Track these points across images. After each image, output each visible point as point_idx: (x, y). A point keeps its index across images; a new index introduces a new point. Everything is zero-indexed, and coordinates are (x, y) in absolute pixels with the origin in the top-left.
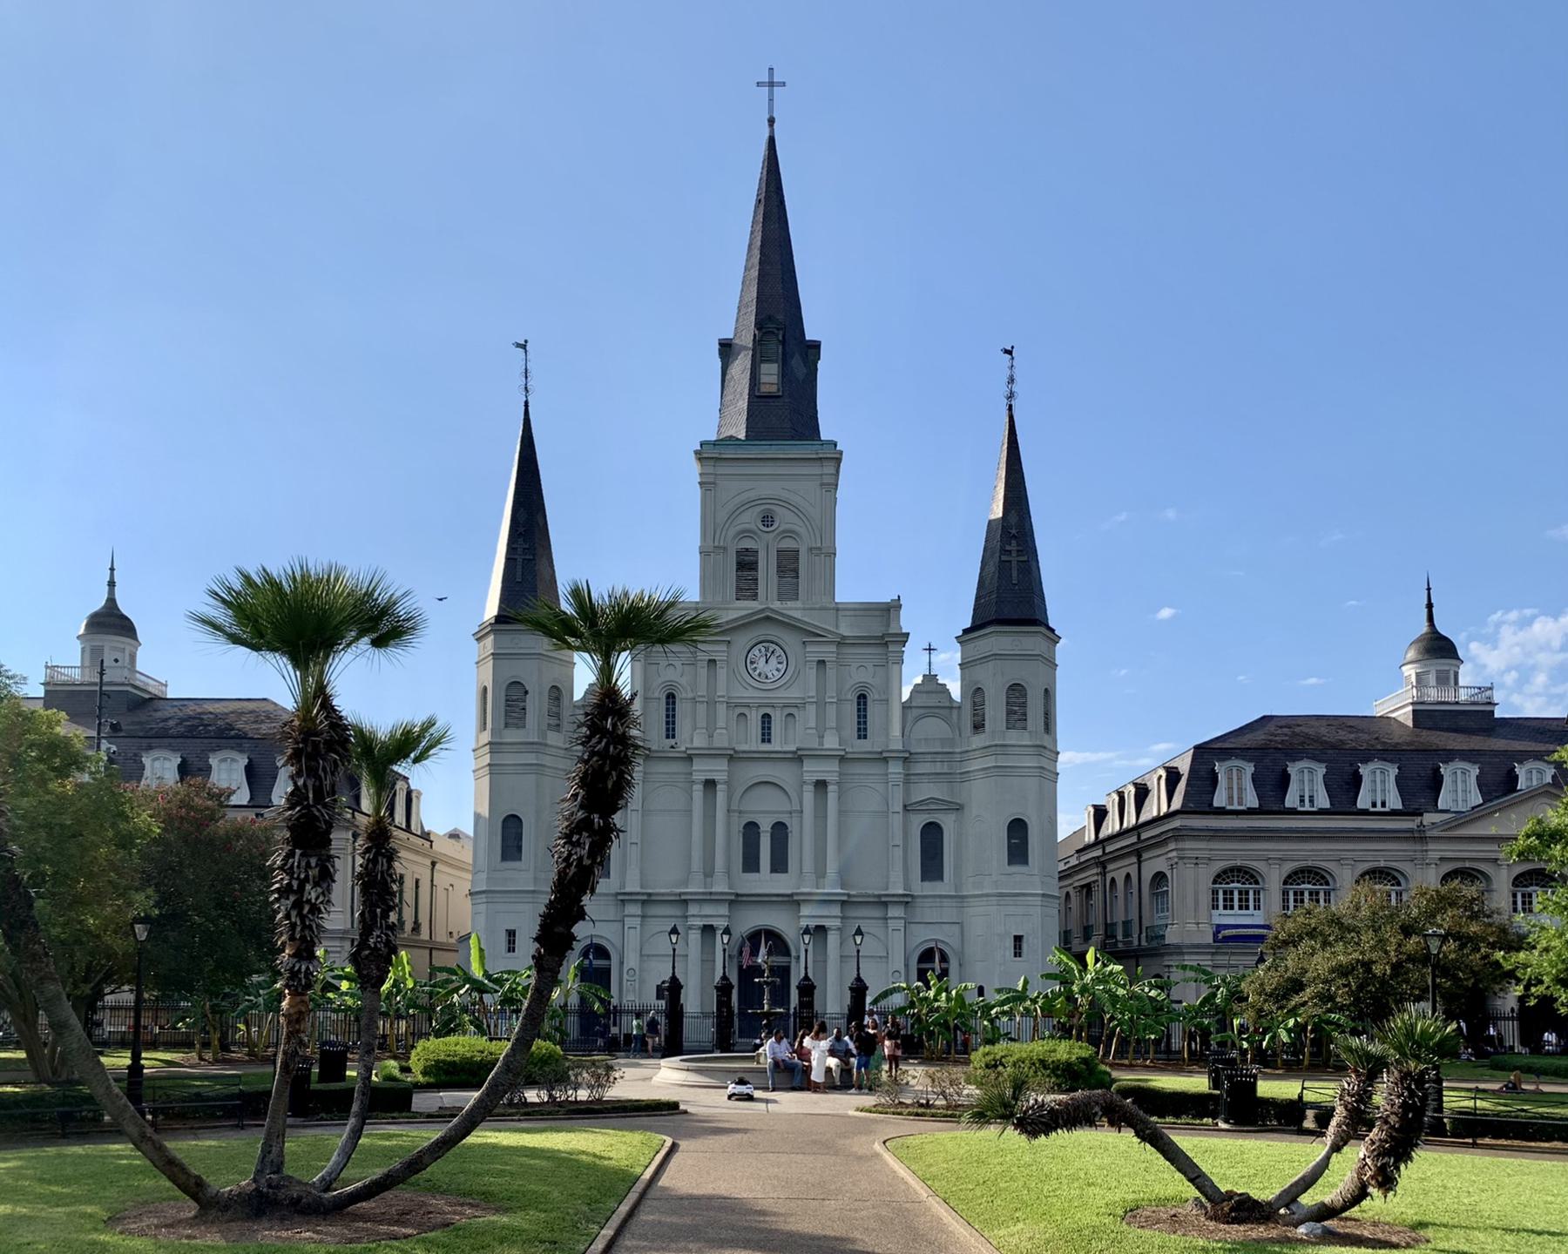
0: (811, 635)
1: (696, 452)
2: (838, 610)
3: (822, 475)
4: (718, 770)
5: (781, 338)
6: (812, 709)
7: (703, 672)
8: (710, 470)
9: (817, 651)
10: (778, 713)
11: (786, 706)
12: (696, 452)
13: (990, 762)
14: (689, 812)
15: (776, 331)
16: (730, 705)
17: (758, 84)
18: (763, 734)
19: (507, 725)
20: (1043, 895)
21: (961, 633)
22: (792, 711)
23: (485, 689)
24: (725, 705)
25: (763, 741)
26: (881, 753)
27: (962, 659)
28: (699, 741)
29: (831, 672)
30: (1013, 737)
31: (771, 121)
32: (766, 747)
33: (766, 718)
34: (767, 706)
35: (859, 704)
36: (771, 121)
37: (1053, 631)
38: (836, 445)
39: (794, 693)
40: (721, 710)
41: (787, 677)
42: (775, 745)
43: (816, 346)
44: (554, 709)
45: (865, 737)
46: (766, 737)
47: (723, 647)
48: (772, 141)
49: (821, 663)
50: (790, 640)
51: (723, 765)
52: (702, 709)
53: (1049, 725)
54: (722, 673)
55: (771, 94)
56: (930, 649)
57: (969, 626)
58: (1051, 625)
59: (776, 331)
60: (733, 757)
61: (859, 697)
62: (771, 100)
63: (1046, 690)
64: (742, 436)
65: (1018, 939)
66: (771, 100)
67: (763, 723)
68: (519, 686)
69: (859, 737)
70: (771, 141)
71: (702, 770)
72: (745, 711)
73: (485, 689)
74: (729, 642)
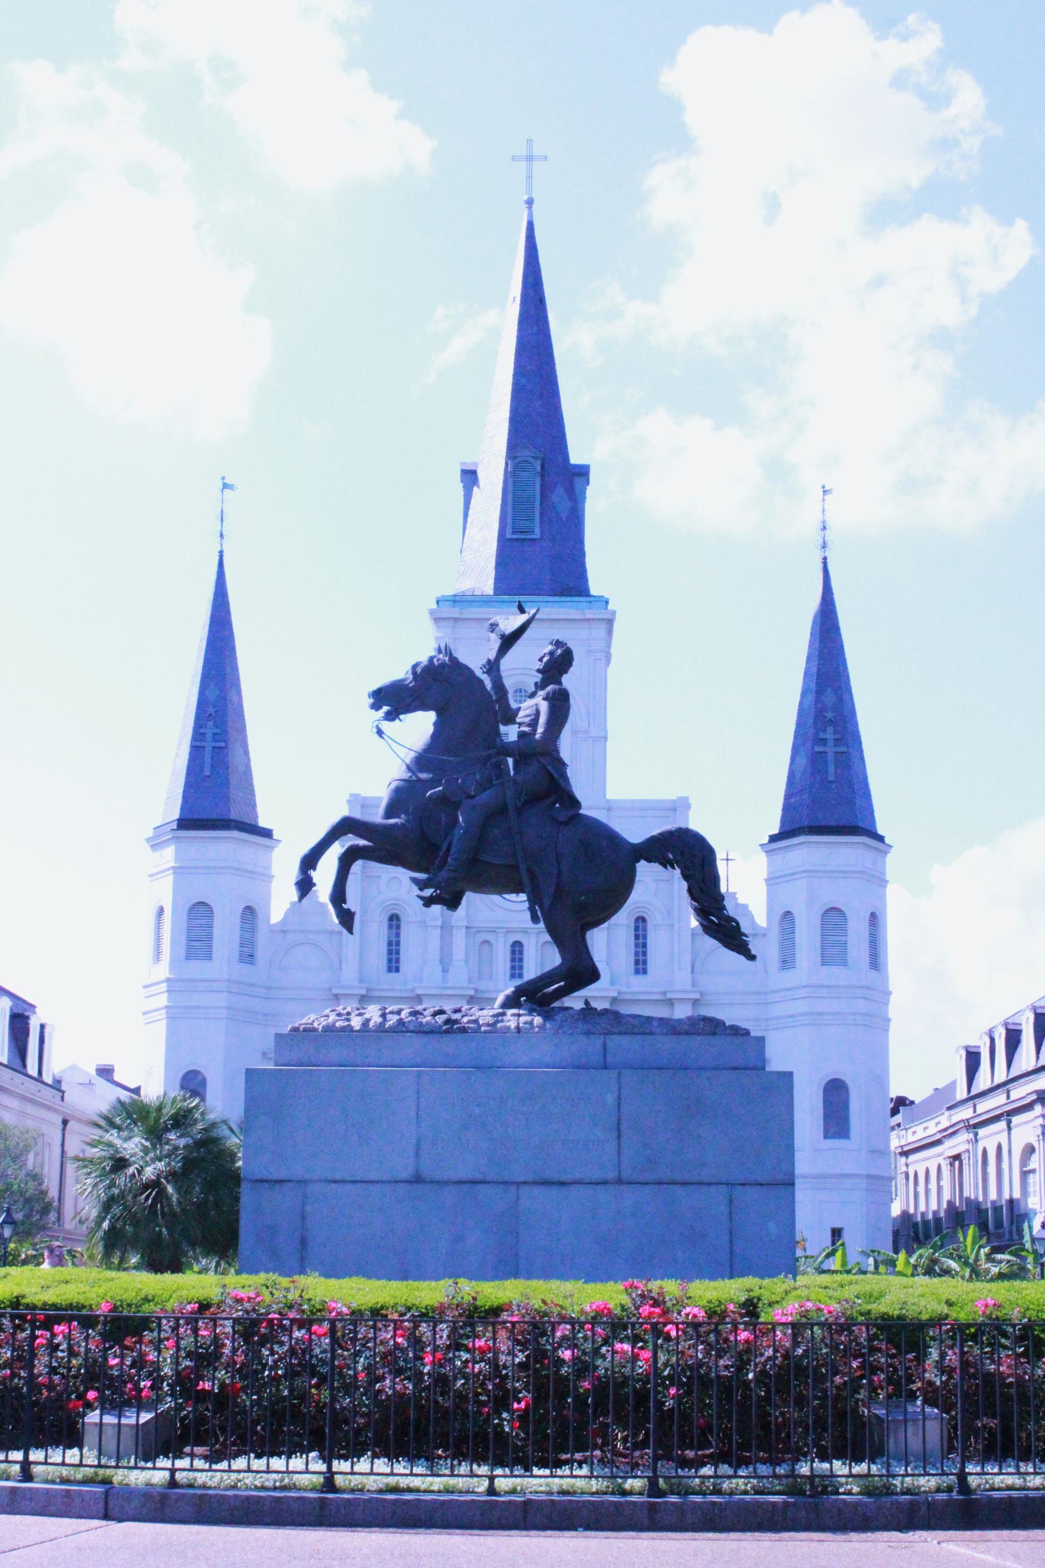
3: (588, 639)
5: (539, 468)
13: (802, 1006)
15: (531, 460)
17: (514, 158)
18: (513, 968)
19: (188, 957)
20: (868, 1176)
21: (766, 840)
23: (161, 911)
24: (464, 930)
26: (665, 993)
27: (769, 873)
30: (834, 975)
31: (530, 203)
35: (636, 928)
36: (530, 203)
37: (881, 839)
38: (607, 602)
43: (583, 472)
44: (247, 935)
45: (645, 972)
48: (530, 227)
53: (876, 959)
56: (727, 860)
57: (776, 831)
58: (880, 832)
59: (531, 460)
61: (637, 920)
62: (529, 177)
64: (490, 590)
65: (836, 1233)
66: (529, 177)
67: (513, 952)
68: (201, 908)
69: (637, 972)
70: (530, 227)
72: (489, 937)
73: (161, 911)
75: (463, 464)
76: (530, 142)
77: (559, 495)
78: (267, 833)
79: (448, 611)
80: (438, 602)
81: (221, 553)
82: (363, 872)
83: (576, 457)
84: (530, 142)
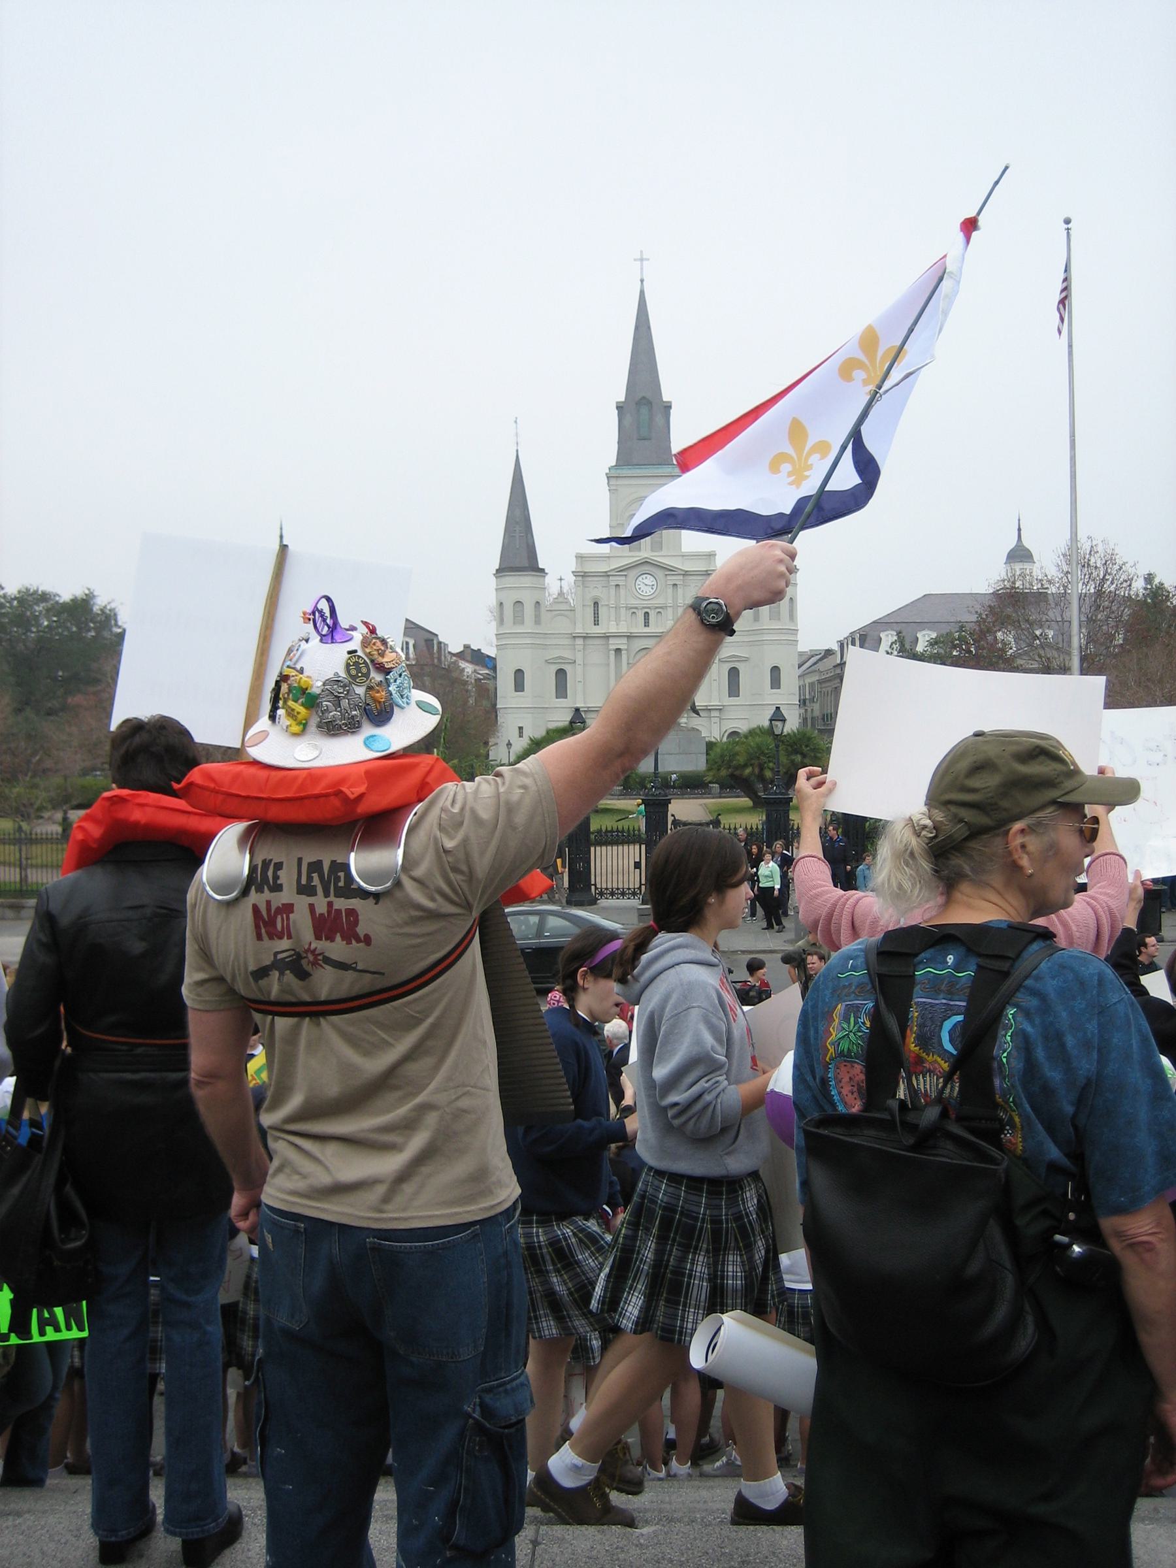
0: (668, 570)
1: (607, 474)
2: (683, 556)
4: (622, 643)
6: (670, 610)
7: (613, 591)
8: (613, 482)
9: (672, 579)
10: (653, 611)
11: (657, 608)
12: (607, 474)
14: (608, 665)
16: (628, 608)
17: (635, 260)
19: (514, 623)
22: (660, 609)
25: (645, 626)
28: (613, 629)
29: (680, 591)
31: (642, 281)
32: (647, 630)
33: (647, 614)
34: (649, 608)
36: (642, 281)
39: (659, 601)
40: (623, 611)
41: (656, 593)
42: (652, 629)
43: (668, 407)
46: (647, 624)
47: (624, 578)
48: (642, 293)
49: (675, 585)
50: (660, 574)
51: (625, 640)
52: (613, 611)
54: (622, 591)
55: (642, 265)
60: (629, 637)
62: (642, 269)
63: (791, 598)
66: (642, 269)
70: (642, 293)
71: (614, 643)
73: (501, 603)
74: (626, 575)
75: (617, 403)
76: (641, 252)
77: (659, 420)
78: (543, 570)
79: (614, 473)
80: (609, 469)
81: (517, 451)
82: (583, 584)
83: (664, 400)
84: (641, 252)
